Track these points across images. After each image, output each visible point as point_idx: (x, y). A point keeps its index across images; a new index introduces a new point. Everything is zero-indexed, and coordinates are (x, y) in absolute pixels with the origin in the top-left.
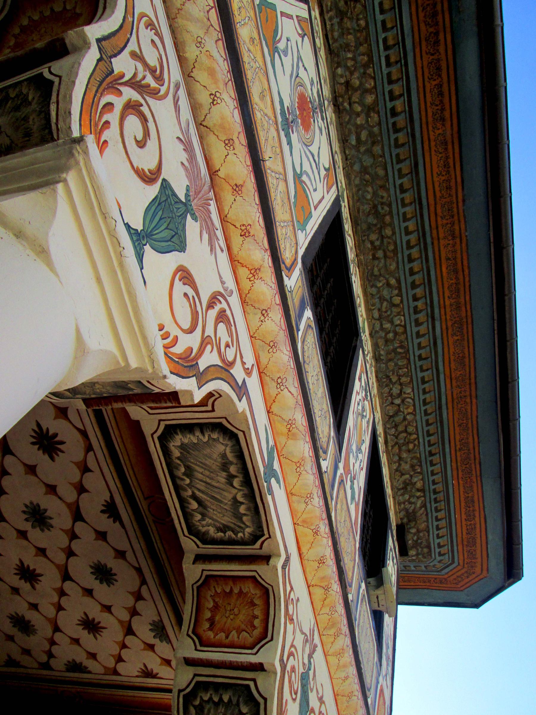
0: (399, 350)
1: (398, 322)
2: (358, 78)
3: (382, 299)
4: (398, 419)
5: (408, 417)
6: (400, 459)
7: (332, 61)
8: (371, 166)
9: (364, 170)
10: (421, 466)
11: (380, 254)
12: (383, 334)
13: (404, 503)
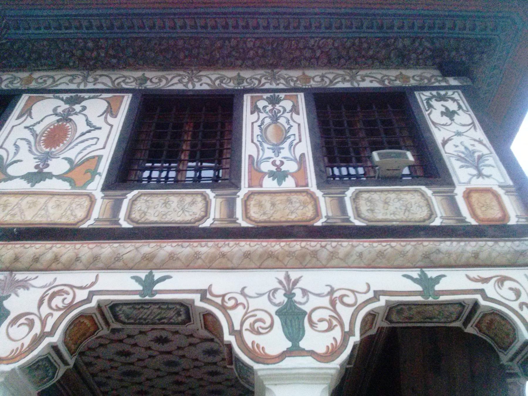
0: (275, 46)
1: (252, 43)
2: (77, 51)
3: (229, 55)
4: (334, 54)
5: (336, 45)
6: (371, 57)
7: (65, 68)
8: (133, 49)
9: (134, 55)
10: (389, 38)
11: (195, 52)
12: (258, 58)
13: (418, 59)
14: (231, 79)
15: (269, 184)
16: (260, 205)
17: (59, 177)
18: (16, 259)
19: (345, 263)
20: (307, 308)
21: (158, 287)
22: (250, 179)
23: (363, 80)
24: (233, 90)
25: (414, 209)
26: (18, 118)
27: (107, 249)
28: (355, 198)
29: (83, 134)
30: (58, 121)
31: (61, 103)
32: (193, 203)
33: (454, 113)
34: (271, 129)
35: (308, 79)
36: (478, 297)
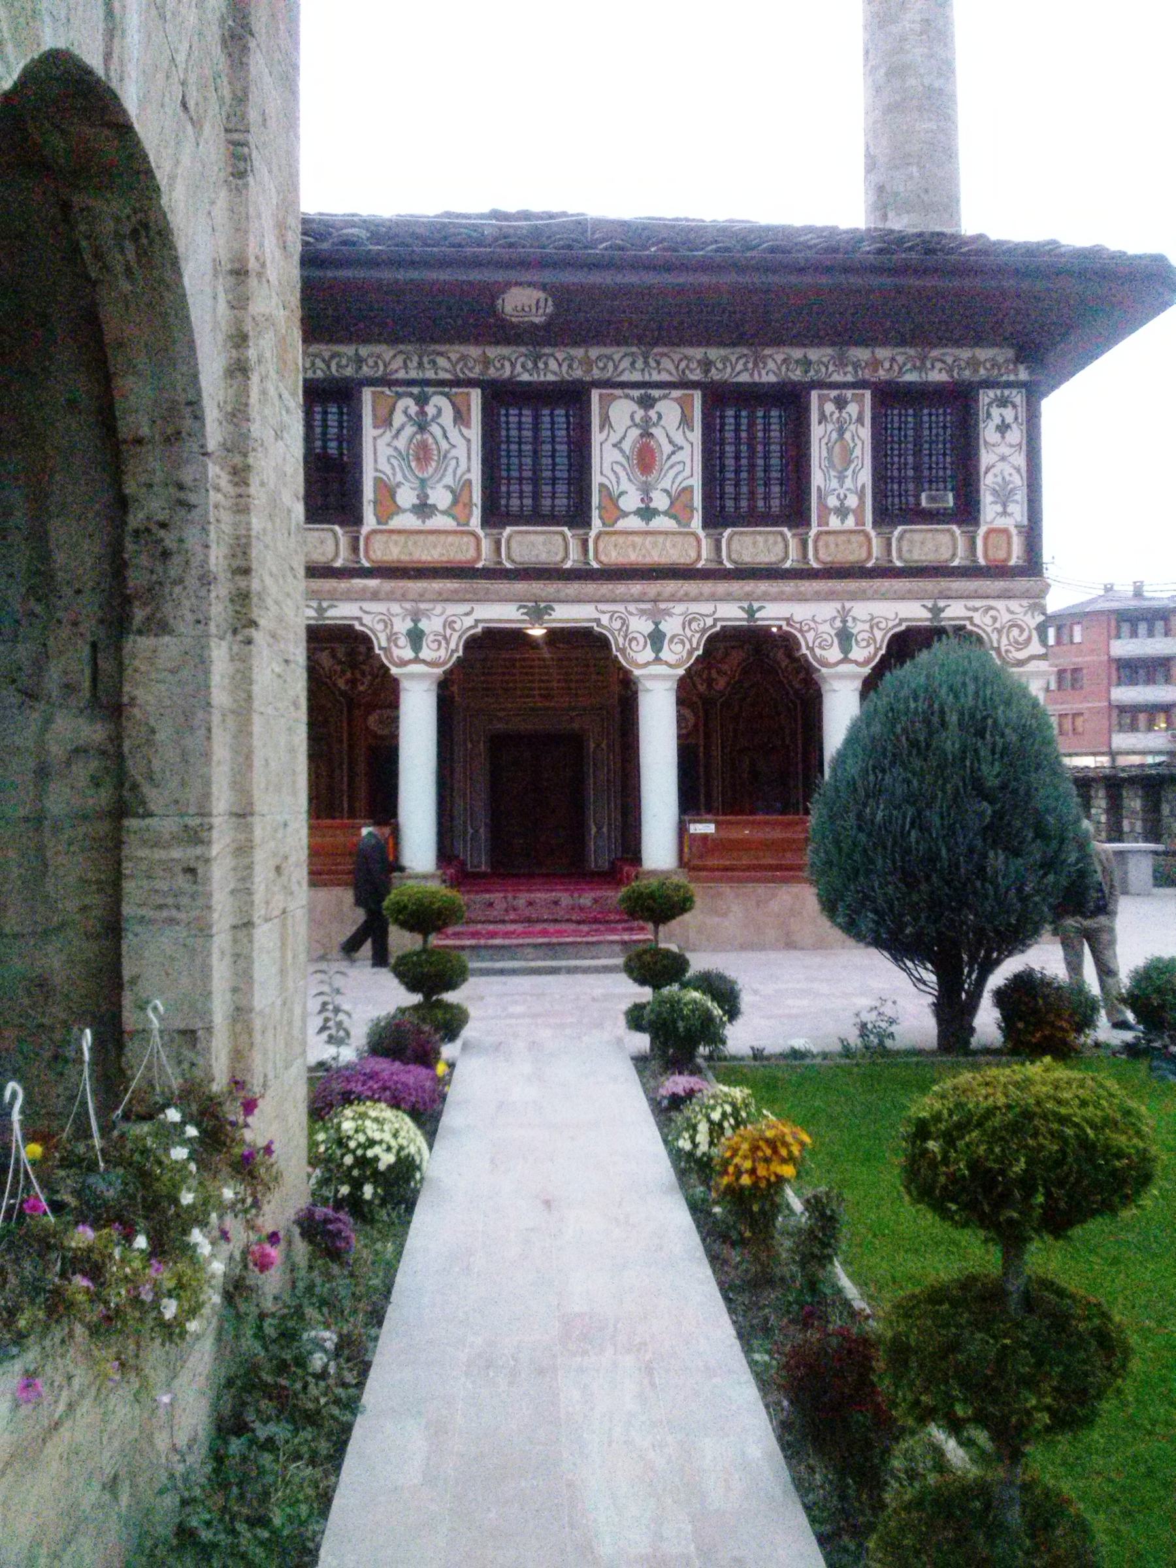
14: (797, 362)
15: (834, 522)
16: (827, 545)
17: (666, 513)
18: (659, 594)
19: (884, 597)
20: (854, 631)
21: (757, 615)
22: (819, 517)
23: (933, 367)
24: (800, 383)
25: (943, 550)
26: (602, 428)
27: (722, 587)
28: (900, 539)
29: (669, 457)
30: (642, 436)
31: (635, 407)
32: (776, 543)
33: (1008, 426)
34: (837, 449)
35: (876, 364)
36: (967, 623)
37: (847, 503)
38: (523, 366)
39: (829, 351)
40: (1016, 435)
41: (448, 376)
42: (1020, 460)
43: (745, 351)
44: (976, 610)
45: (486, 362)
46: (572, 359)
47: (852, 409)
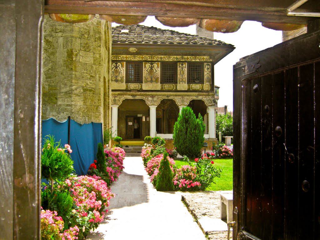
24: (176, 61)
26: (144, 68)
35: (188, 58)
37: (183, 80)
38: (132, 58)
39: (180, 56)
40: (209, 70)
41: (120, 60)
42: (211, 74)
43: (167, 56)
44: (203, 97)
45: (126, 58)
46: (140, 57)
47: (184, 65)
